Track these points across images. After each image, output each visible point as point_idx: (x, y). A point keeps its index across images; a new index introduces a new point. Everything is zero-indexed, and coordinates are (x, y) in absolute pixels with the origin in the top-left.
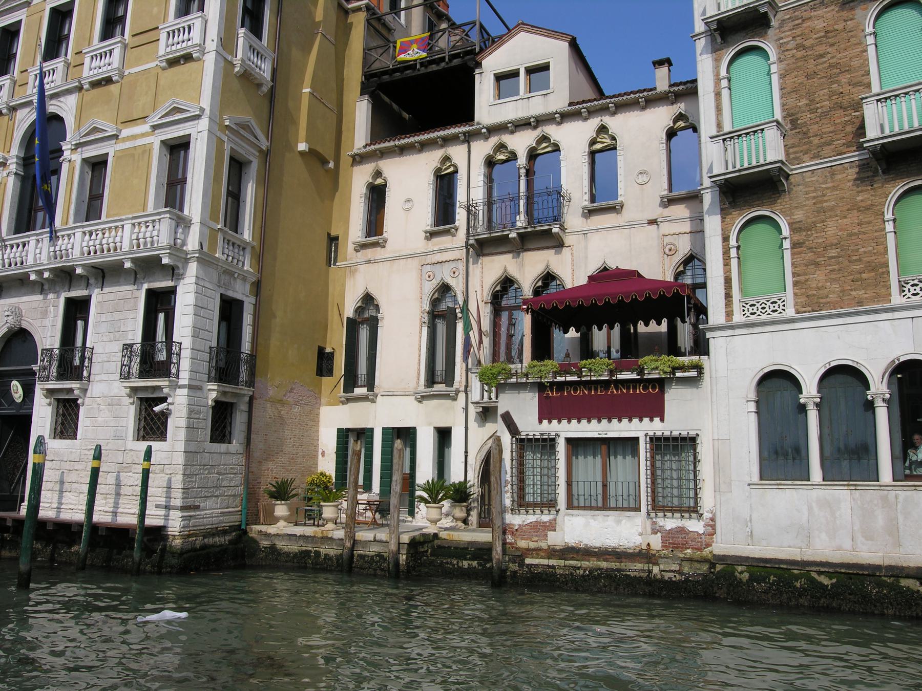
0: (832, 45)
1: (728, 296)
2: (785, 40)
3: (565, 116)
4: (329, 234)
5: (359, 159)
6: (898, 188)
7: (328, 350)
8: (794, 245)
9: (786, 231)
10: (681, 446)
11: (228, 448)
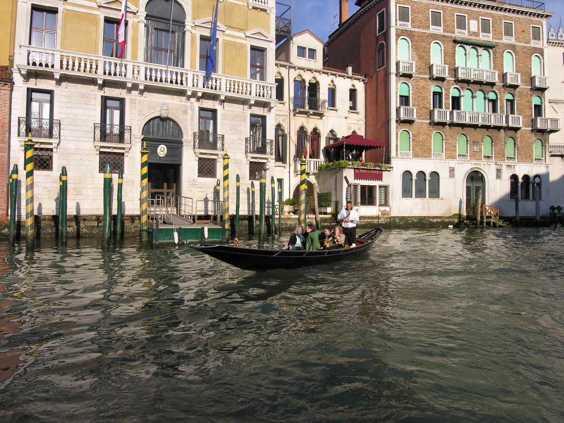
1: (397, 150)
8: (413, 140)
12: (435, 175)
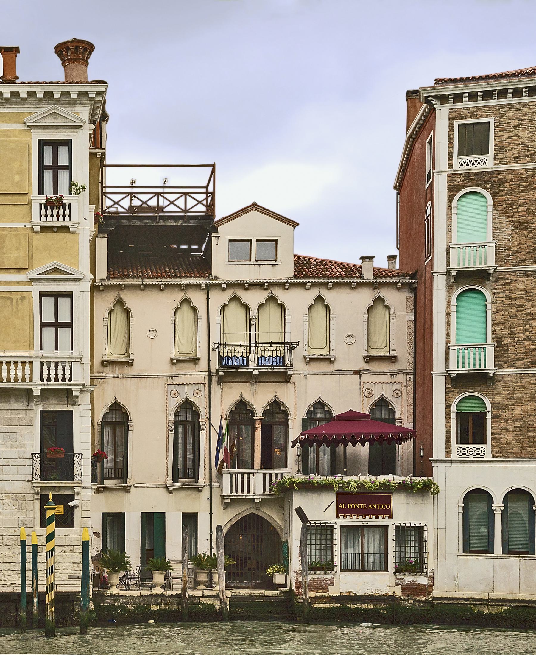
2: (498, 291)
9: (489, 408)
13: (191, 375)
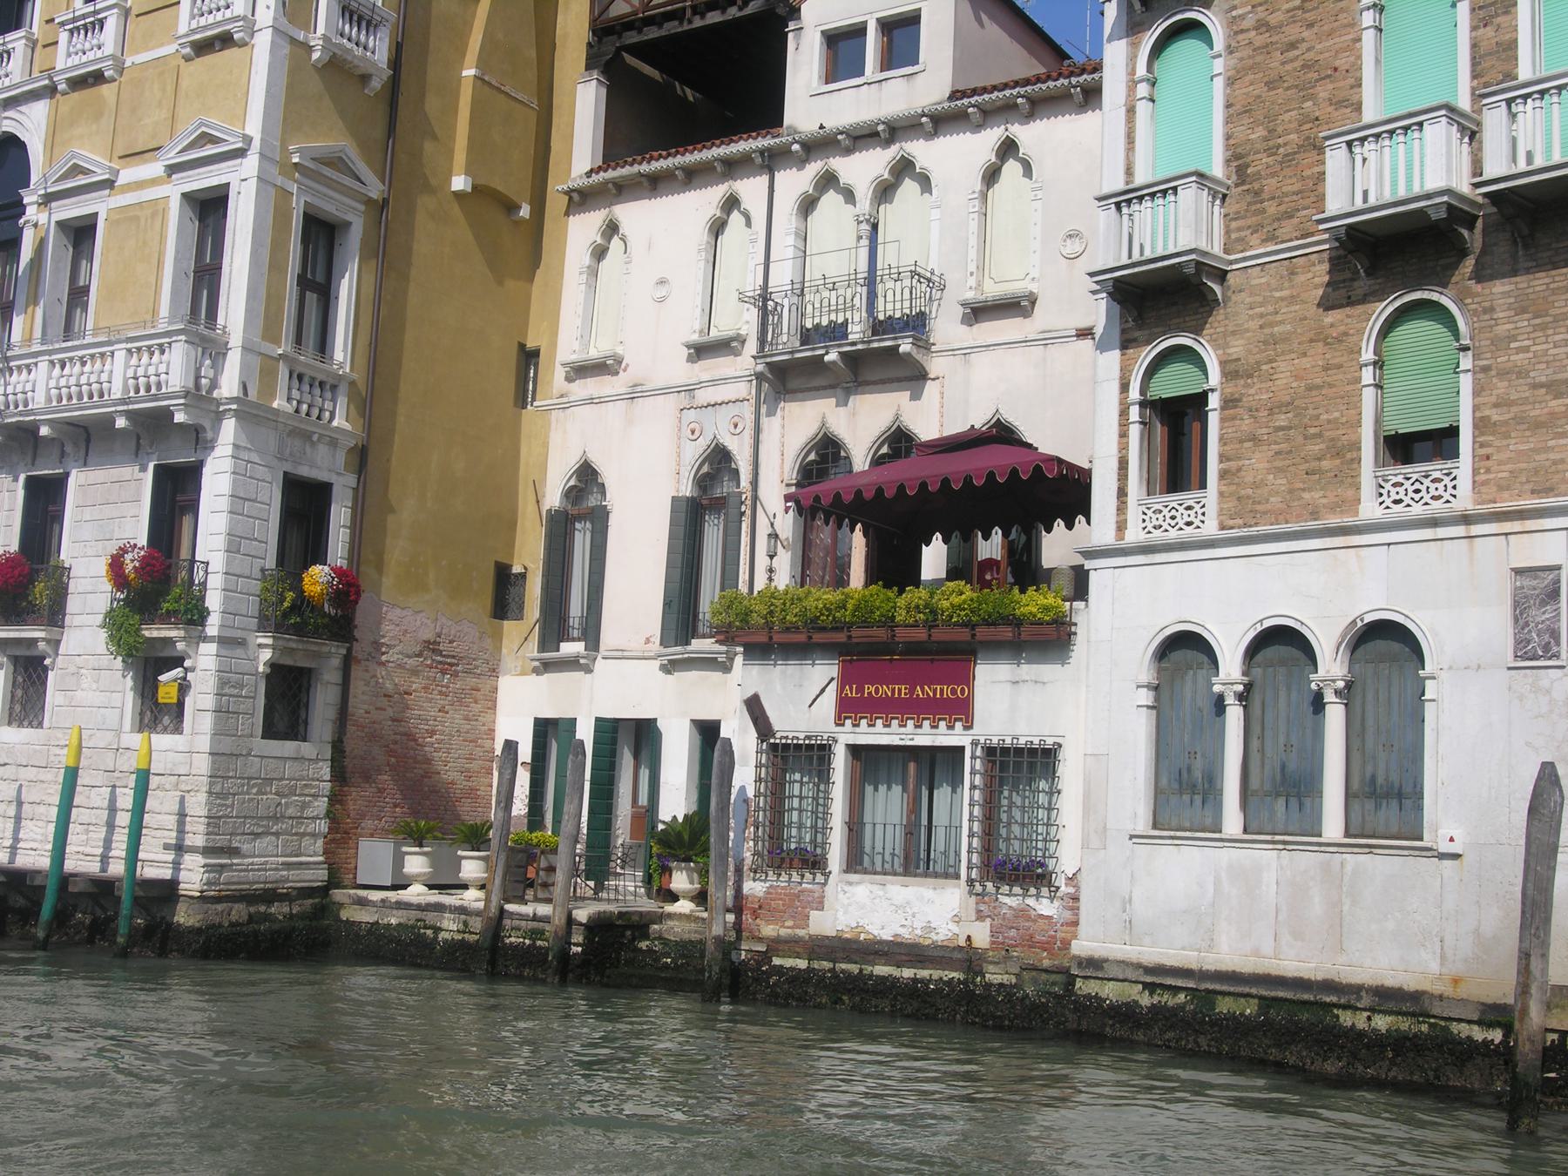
0: (1310, 25)
3: (940, 122)
4: (522, 346)
5: (581, 199)
6: (1383, 309)
7: (517, 569)
10: (1024, 766)
11: (298, 751)
12: (1385, 642)
13: (725, 380)
